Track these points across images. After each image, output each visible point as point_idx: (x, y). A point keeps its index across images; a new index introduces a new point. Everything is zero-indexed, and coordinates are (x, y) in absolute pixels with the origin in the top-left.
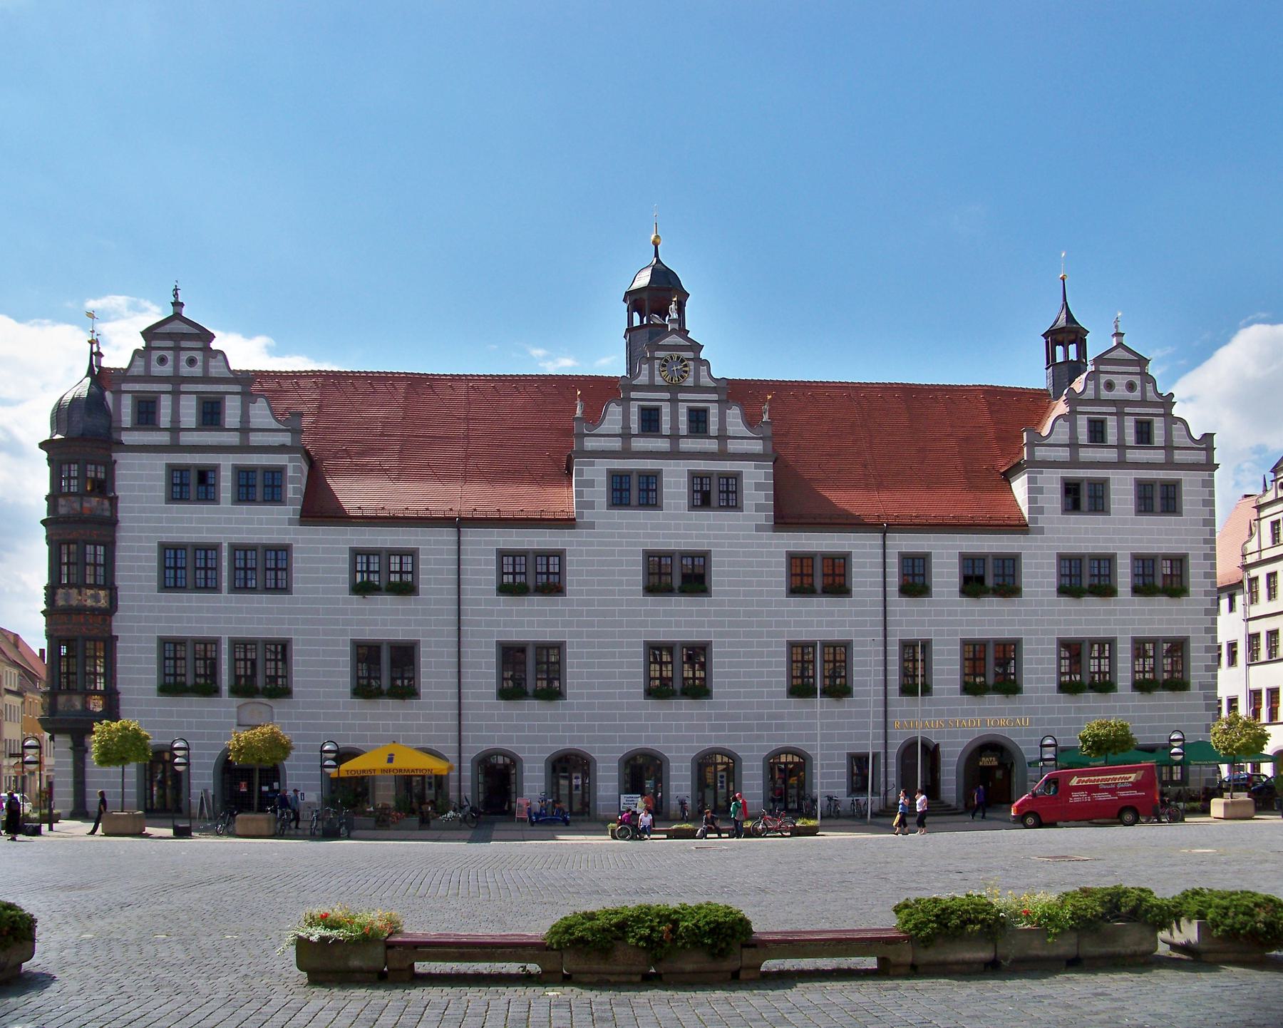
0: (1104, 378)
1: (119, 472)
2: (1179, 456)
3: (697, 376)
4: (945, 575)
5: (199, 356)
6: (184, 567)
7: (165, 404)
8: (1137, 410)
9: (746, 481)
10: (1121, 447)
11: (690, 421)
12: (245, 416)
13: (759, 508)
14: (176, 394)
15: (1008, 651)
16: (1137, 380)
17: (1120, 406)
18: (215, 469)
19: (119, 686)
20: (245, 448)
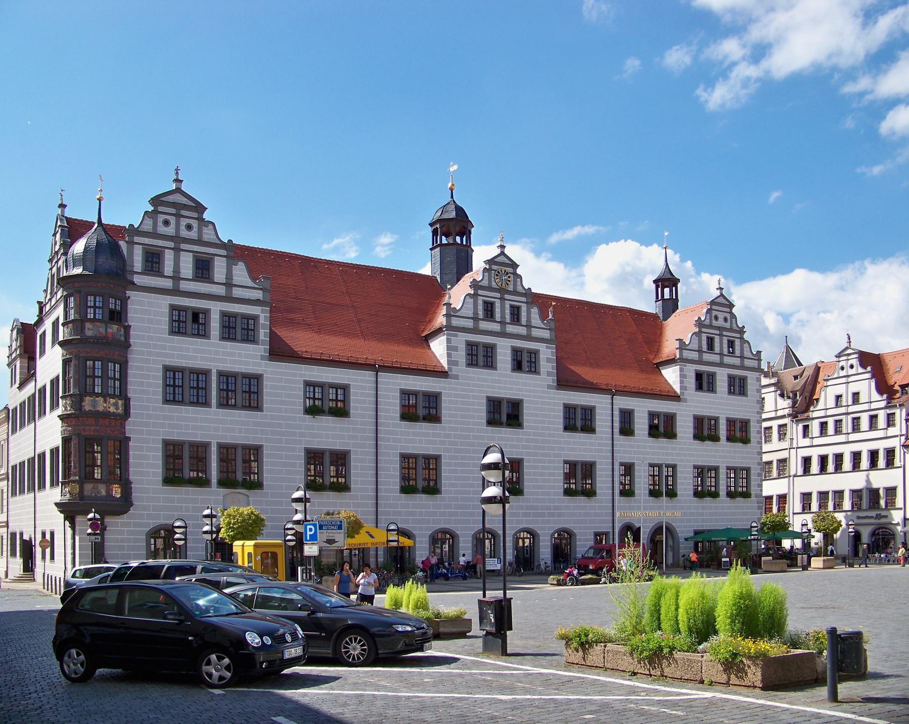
1: (130, 306)
3: (515, 285)
4: (641, 424)
5: (195, 223)
6: (184, 386)
7: (169, 256)
11: (512, 314)
12: (229, 275)
13: (549, 374)
14: (177, 250)
16: (728, 316)
18: (206, 312)
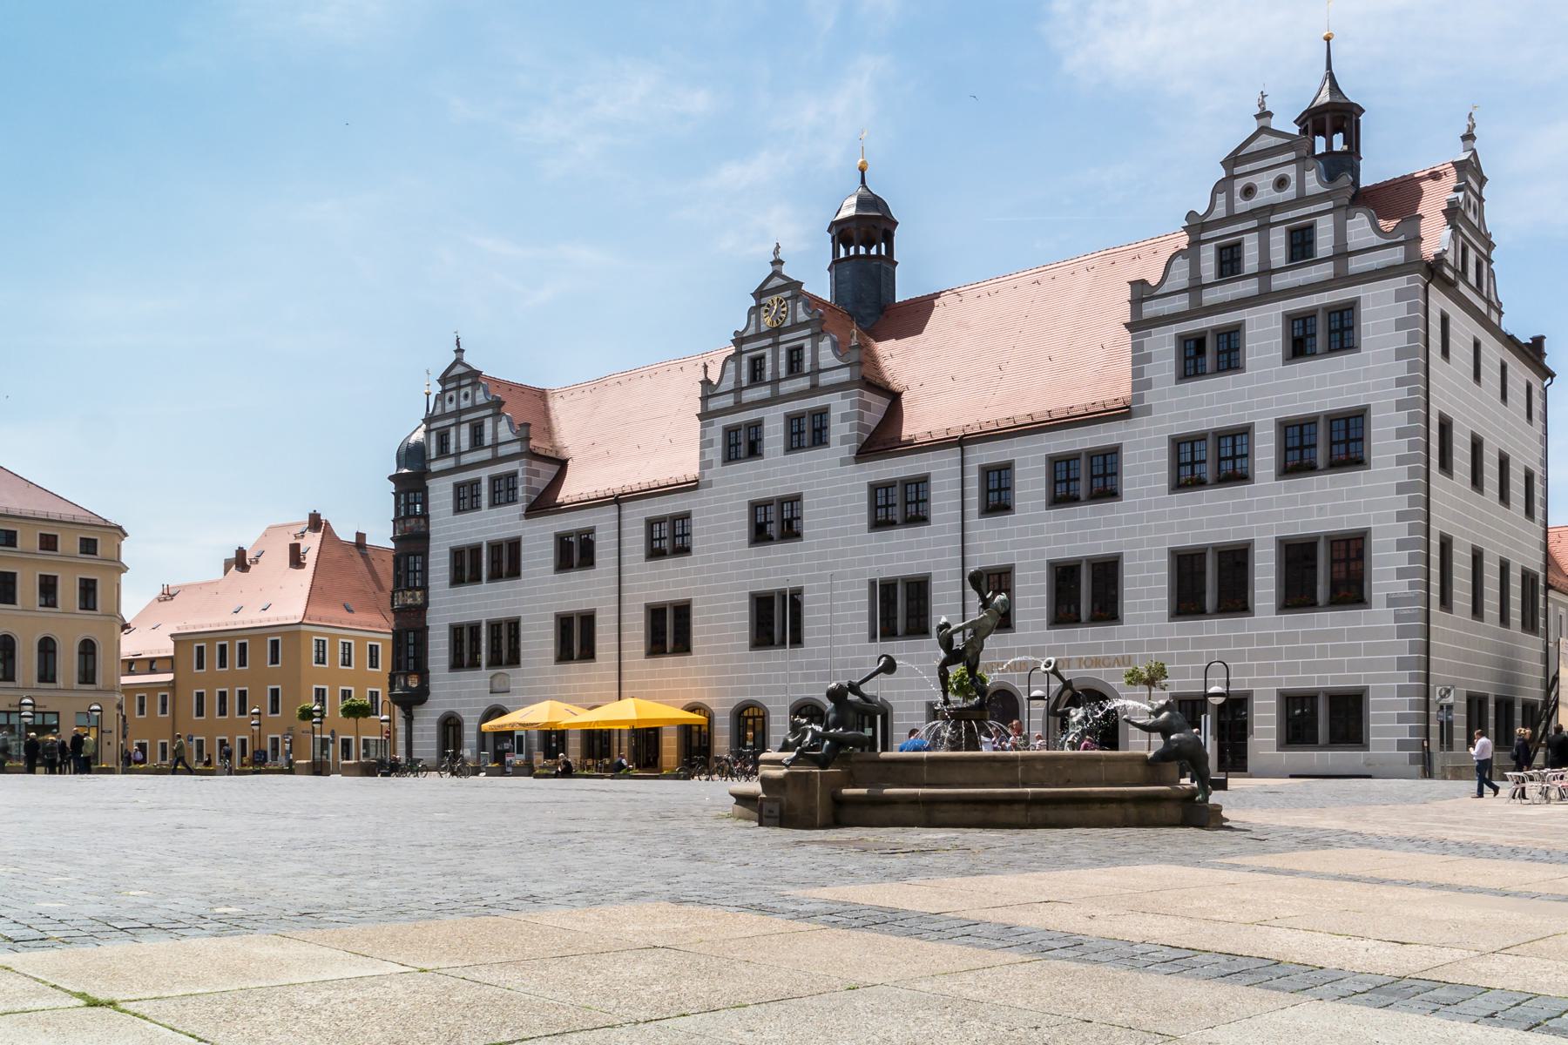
0: (1239, 185)
2: (1356, 265)
8: (1290, 214)
9: (834, 415)
13: (844, 440)
17: (1263, 217)
19: (430, 666)
20: (496, 460)
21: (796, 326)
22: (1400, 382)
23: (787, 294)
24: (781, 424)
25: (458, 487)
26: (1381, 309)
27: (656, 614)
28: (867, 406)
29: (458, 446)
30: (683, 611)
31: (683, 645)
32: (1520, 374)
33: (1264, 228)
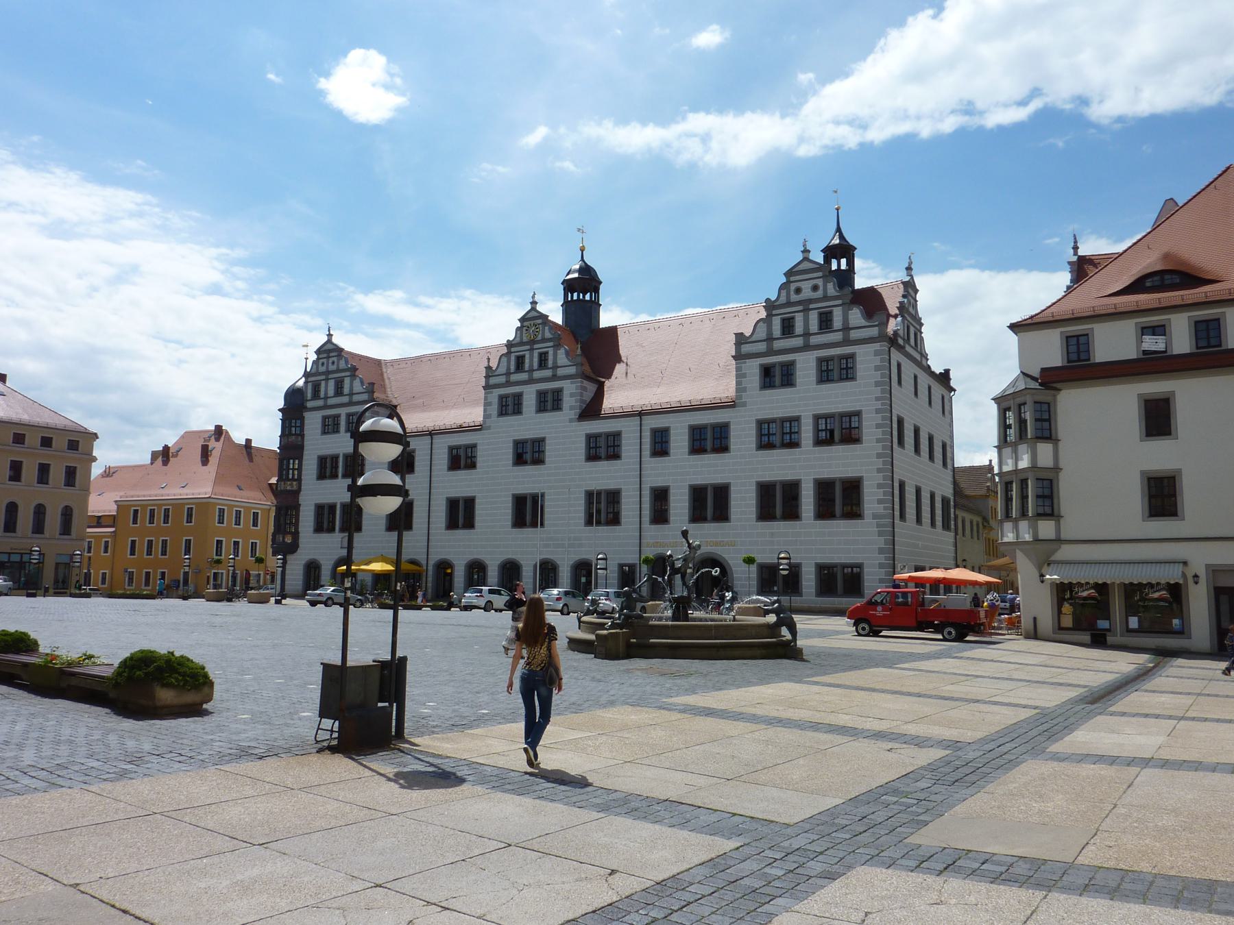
2: (854, 335)
9: (566, 393)
10: (807, 334)
13: (571, 408)
15: (721, 493)
17: (806, 305)
20: (351, 404)
21: (544, 340)
22: (877, 399)
23: (540, 321)
24: (534, 396)
25: (324, 418)
26: (867, 359)
27: (453, 504)
28: (584, 389)
29: (326, 393)
30: (470, 503)
31: (469, 524)
32: (938, 390)
33: (806, 310)
